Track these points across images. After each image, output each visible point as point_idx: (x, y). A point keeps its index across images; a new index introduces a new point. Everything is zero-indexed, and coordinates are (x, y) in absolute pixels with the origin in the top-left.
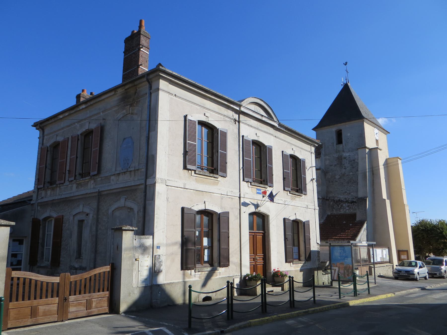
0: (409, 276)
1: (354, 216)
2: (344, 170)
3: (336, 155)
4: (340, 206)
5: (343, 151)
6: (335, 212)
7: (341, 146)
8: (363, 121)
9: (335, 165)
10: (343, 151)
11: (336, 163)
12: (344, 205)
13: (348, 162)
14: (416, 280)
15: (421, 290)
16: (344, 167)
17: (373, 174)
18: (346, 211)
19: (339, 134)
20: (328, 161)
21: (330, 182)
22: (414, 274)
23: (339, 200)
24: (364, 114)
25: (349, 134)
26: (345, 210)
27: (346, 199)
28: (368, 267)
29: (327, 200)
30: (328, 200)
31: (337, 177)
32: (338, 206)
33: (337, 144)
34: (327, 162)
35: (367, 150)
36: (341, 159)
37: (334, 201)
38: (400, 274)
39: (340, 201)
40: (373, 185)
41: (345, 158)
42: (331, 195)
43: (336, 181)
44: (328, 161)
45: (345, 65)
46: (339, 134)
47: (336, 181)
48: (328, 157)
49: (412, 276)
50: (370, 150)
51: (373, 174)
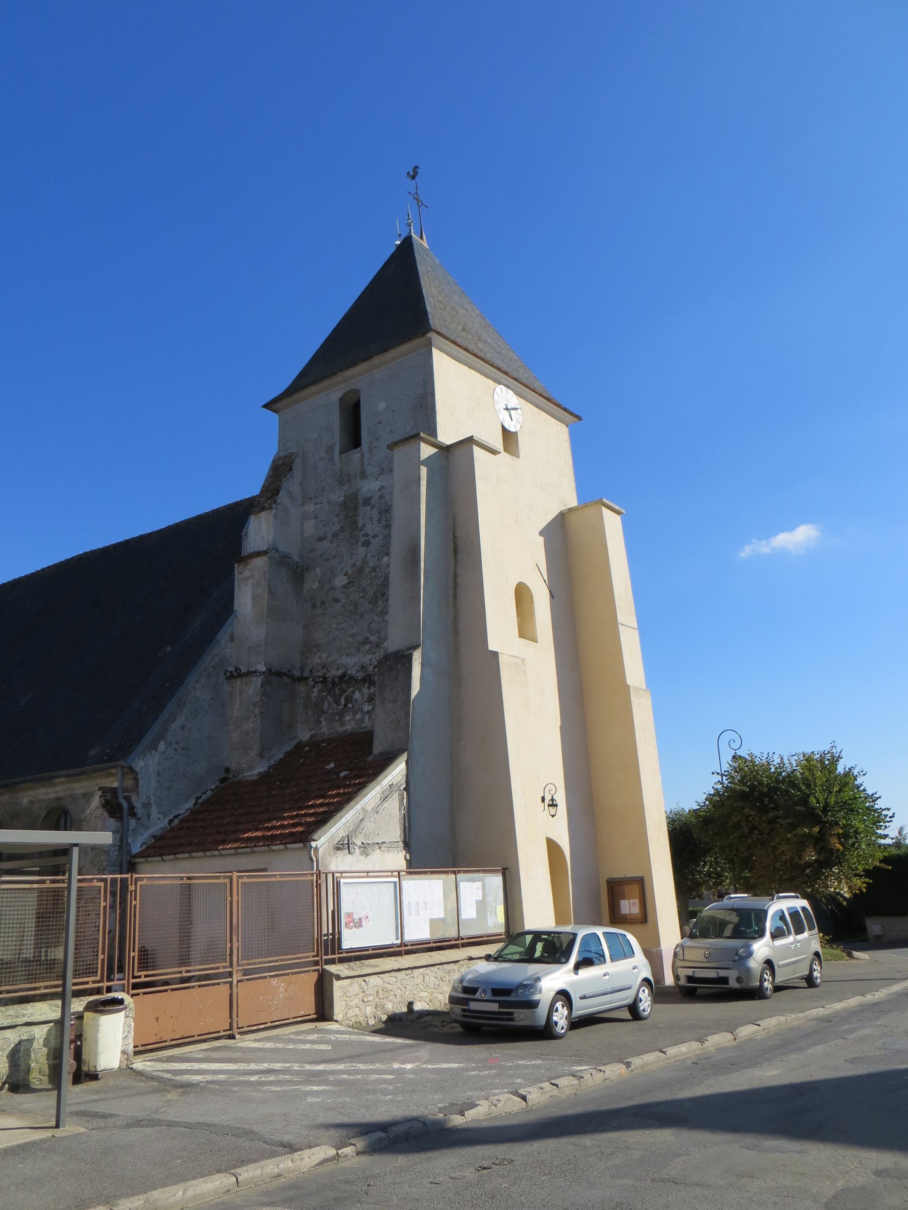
0: (510, 1017)
1: (364, 739)
2: (361, 551)
3: (338, 496)
4: (343, 701)
5: (363, 476)
6: (325, 729)
7: (355, 455)
8: (429, 345)
9: (335, 535)
10: (363, 476)
11: (337, 528)
12: (357, 695)
13: (375, 514)
14: (546, 1032)
15: (373, 1149)
16: (362, 539)
17: (456, 551)
18: (362, 720)
19: (352, 412)
20: (312, 522)
21: (314, 606)
22: (533, 1005)
23: (343, 676)
24: (434, 320)
25: (382, 406)
26: (359, 716)
27: (363, 668)
28: (315, 976)
29: (302, 679)
30: (306, 679)
31: (340, 581)
32: (337, 702)
33: (342, 452)
34: (310, 528)
35: (427, 451)
36: (355, 508)
37: (324, 680)
38: (474, 1006)
39: (345, 679)
40: (455, 597)
41: (367, 502)
42: (317, 661)
43: (336, 600)
44: (312, 522)
45: (413, 177)
46: (352, 412)
47: (336, 600)
48: (311, 507)
49: (521, 1017)
50: (446, 450)
51: (456, 551)
